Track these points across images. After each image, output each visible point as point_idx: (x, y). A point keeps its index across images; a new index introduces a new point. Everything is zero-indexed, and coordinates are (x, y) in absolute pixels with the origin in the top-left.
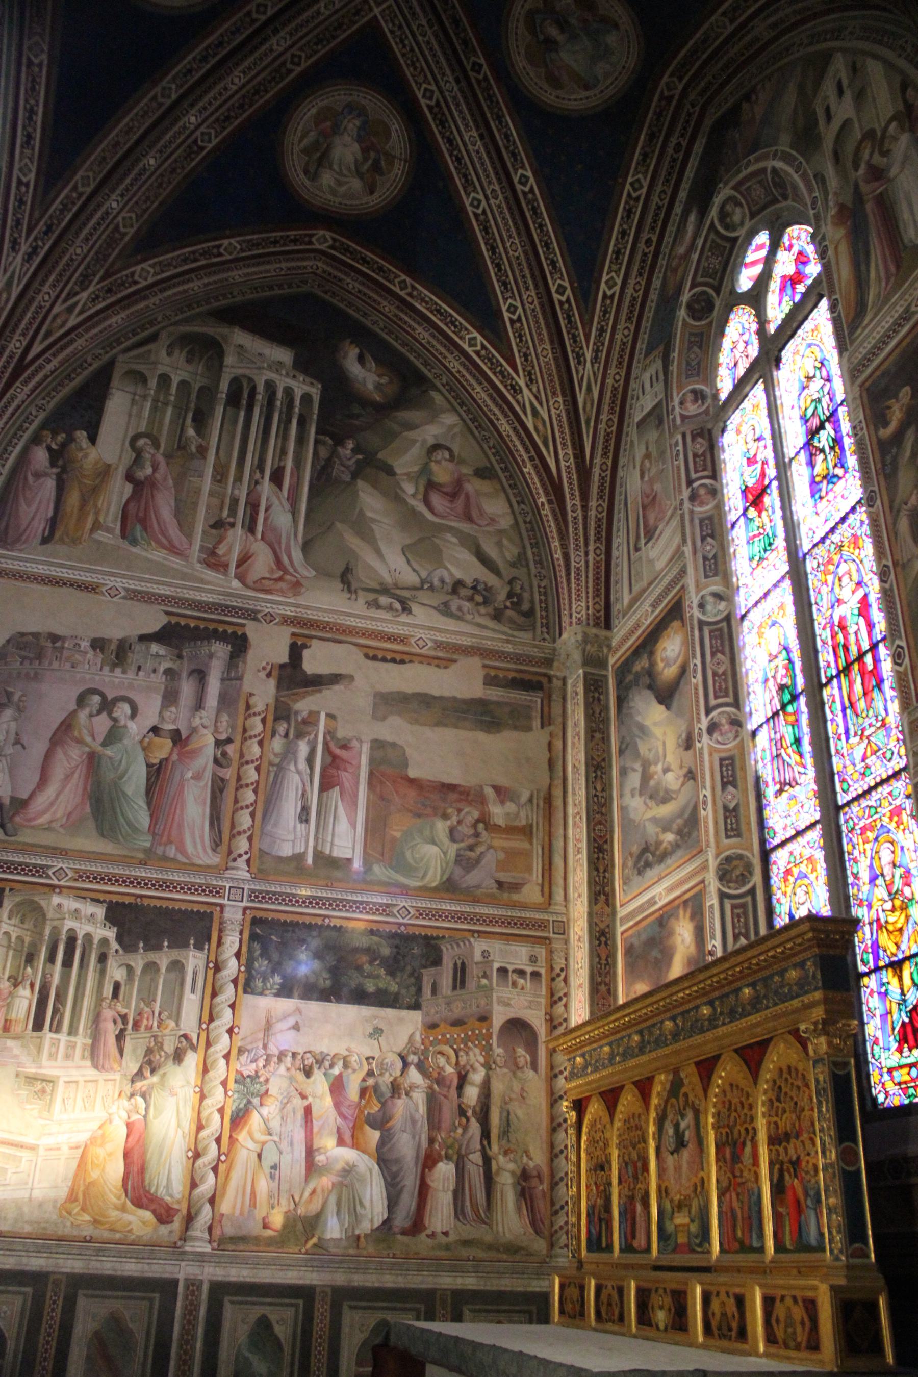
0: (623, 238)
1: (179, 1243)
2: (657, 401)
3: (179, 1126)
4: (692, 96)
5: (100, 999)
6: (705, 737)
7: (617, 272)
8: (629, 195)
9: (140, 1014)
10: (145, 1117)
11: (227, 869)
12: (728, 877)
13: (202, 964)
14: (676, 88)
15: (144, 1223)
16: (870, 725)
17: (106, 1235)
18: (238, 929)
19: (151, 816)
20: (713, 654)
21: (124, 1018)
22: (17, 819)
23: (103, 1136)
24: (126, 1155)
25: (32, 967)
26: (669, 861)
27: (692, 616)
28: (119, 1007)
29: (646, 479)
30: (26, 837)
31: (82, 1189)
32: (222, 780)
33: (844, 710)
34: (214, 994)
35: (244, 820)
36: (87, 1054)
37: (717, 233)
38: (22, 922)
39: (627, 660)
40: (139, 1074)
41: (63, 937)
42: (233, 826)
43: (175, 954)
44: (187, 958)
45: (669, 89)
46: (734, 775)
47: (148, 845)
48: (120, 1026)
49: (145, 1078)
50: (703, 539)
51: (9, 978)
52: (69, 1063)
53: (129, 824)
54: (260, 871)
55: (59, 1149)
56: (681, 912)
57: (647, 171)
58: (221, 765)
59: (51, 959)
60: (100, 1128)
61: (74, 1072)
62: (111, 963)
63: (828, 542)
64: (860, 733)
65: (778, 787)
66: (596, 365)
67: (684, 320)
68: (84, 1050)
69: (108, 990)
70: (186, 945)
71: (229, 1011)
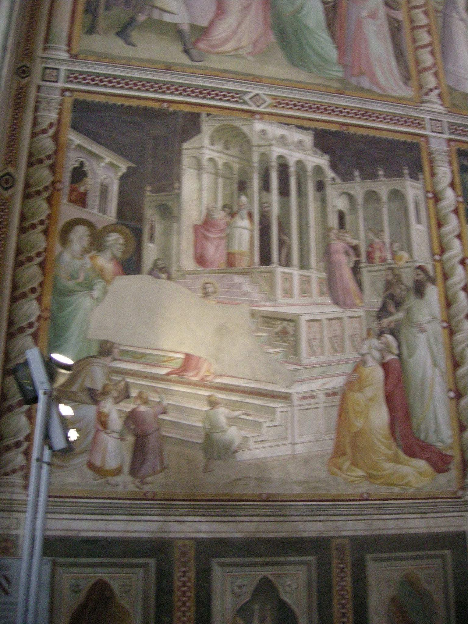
1: (460, 493)
3: (435, 365)
5: (326, 231)
9: (371, 245)
10: (399, 355)
11: (423, 102)
13: (420, 194)
15: (420, 473)
17: (385, 491)
18: (447, 159)
19: (338, 48)
21: (355, 249)
22: (202, 45)
23: (360, 379)
24: (389, 399)
25: (247, 196)
28: (349, 239)
30: (214, 63)
31: (348, 440)
32: (396, 20)
34: (440, 225)
35: (427, 59)
36: (325, 289)
38: (227, 147)
40: (383, 312)
41: (274, 164)
42: (417, 63)
43: (393, 184)
44: (404, 188)
47: (341, 75)
48: (355, 258)
49: (391, 314)
51: (224, 207)
52: (306, 300)
53: (318, 54)
54: (454, 106)
55: (314, 397)
58: (392, 8)
59: (266, 186)
60: (355, 370)
61: (315, 310)
62: (331, 191)
68: (320, 284)
69: (333, 221)
70: (400, 175)
71: (456, 243)
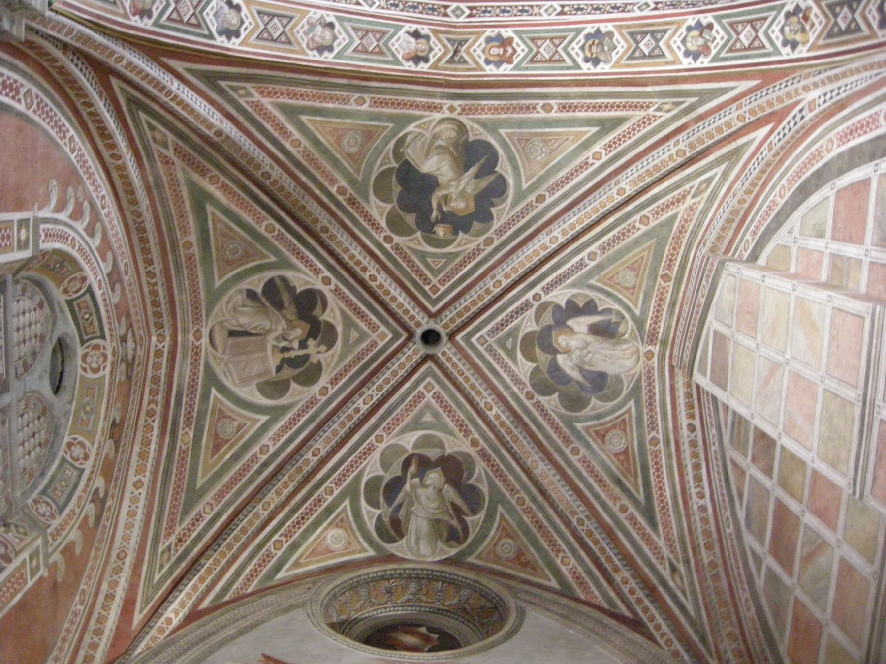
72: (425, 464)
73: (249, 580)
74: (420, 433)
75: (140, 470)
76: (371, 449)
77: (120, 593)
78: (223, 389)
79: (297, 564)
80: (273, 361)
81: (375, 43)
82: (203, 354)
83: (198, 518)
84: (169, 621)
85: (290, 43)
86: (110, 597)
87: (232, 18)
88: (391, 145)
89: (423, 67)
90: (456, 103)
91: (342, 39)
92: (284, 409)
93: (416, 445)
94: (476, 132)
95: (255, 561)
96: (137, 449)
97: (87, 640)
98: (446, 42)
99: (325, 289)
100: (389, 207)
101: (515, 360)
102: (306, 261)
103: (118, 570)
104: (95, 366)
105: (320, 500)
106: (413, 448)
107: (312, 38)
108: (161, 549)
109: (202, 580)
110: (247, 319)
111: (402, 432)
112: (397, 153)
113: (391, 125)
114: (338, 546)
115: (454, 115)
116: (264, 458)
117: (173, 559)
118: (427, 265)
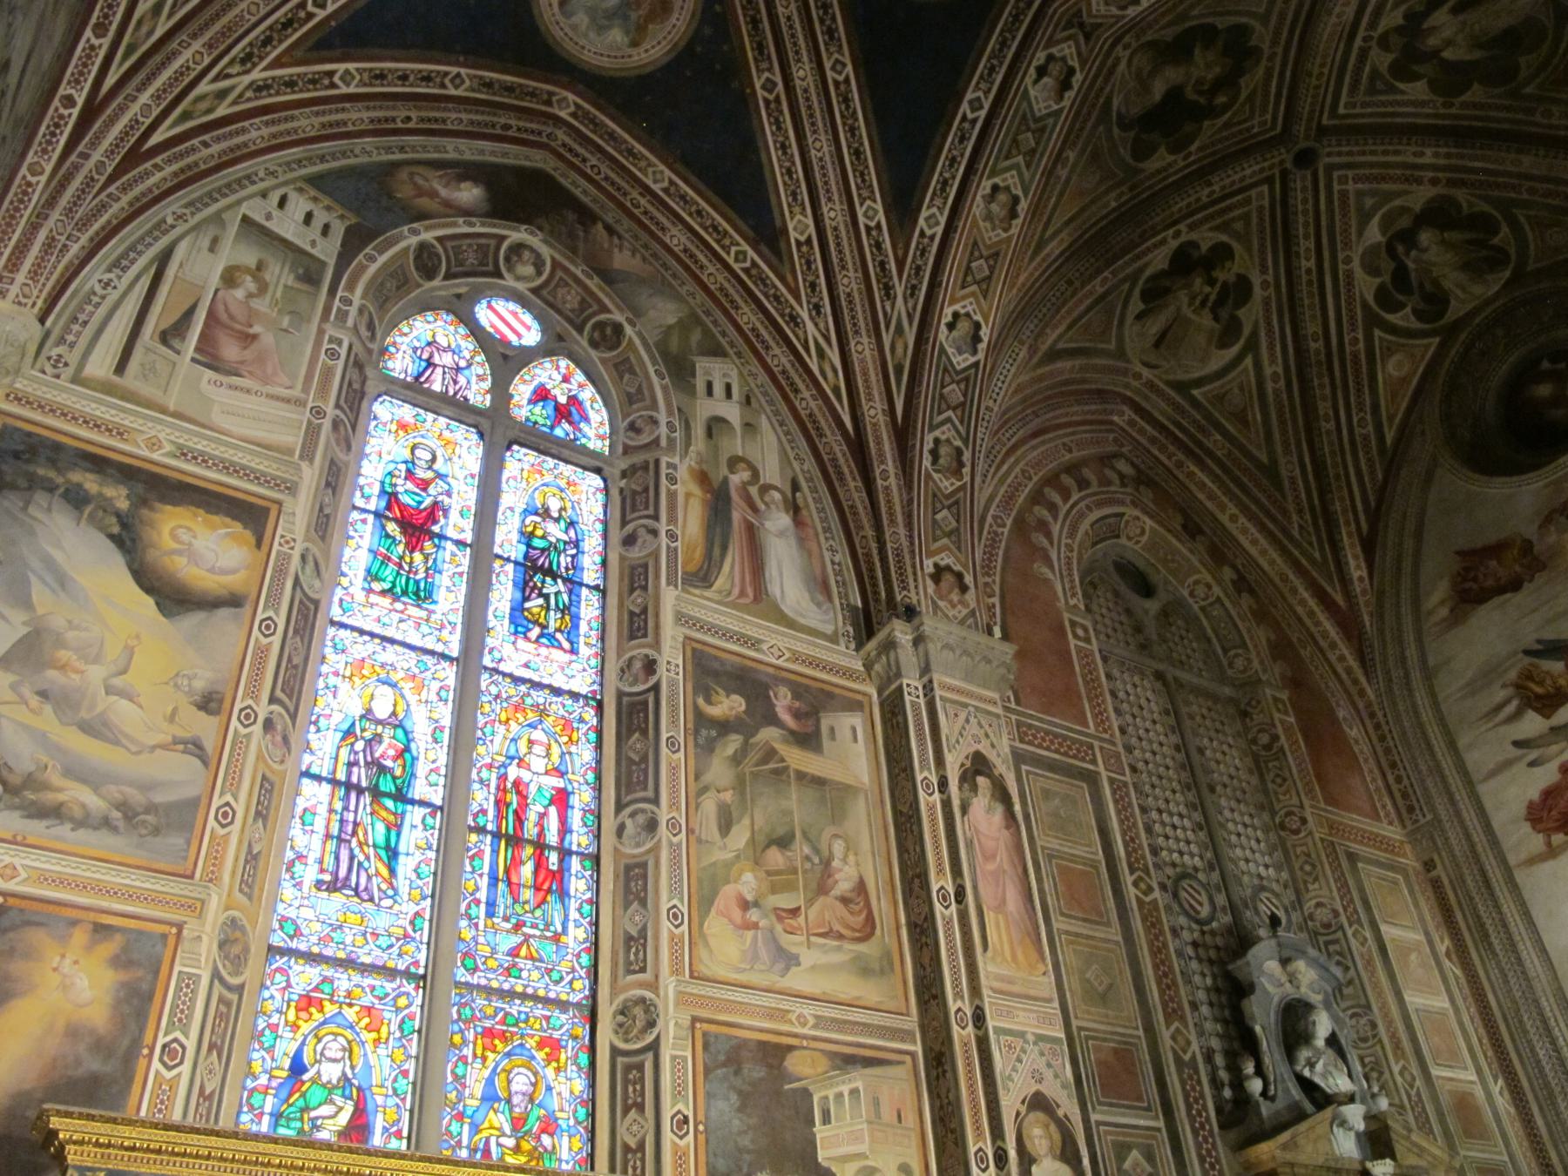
0: (400, 78)
2: (308, 248)
4: (561, 135)
6: (258, 728)
7: (362, 83)
8: (446, 74)
12: (227, 947)
14: (561, 109)
16: (534, 926)
20: (296, 631)
26: (65, 830)
27: (290, 556)
29: (239, 293)
33: (494, 880)
37: (498, 248)
39: (57, 447)
45: (559, 101)
46: (267, 808)
50: (328, 484)
56: (80, 936)
57: (473, 90)
63: (523, 688)
64: (514, 921)
65: (327, 877)
66: (249, 94)
67: (408, 248)
72: (1407, 238)
73: (1372, 472)
74: (1376, 220)
75: (1223, 508)
76: (1349, 275)
77: (1312, 603)
78: (1199, 383)
79: (1391, 418)
80: (1206, 320)
81: (1029, 135)
82: (1157, 381)
83: (1293, 480)
84: (1361, 579)
85: (997, 254)
86: (1311, 614)
87: (964, 327)
88: (1116, 131)
89: (1077, 79)
90: (1127, 39)
91: (1010, 179)
92: (1254, 334)
93: (1384, 232)
94: (1169, 34)
95: (1361, 454)
96: (1201, 496)
97: (1333, 658)
98: (1066, 33)
99: (1183, 238)
100: (1162, 150)
101: (1402, 92)
102: (1149, 250)
103: (1294, 591)
104: (1138, 531)
105: (1355, 356)
106: (1384, 234)
107: (1001, 221)
108: (1296, 533)
109: (1347, 523)
110: (1154, 327)
111: (1360, 234)
112: (1124, 125)
113: (1101, 128)
114: (1405, 371)
115: (1134, 45)
116: (1282, 383)
117: (1311, 529)
118: (1239, 123)
